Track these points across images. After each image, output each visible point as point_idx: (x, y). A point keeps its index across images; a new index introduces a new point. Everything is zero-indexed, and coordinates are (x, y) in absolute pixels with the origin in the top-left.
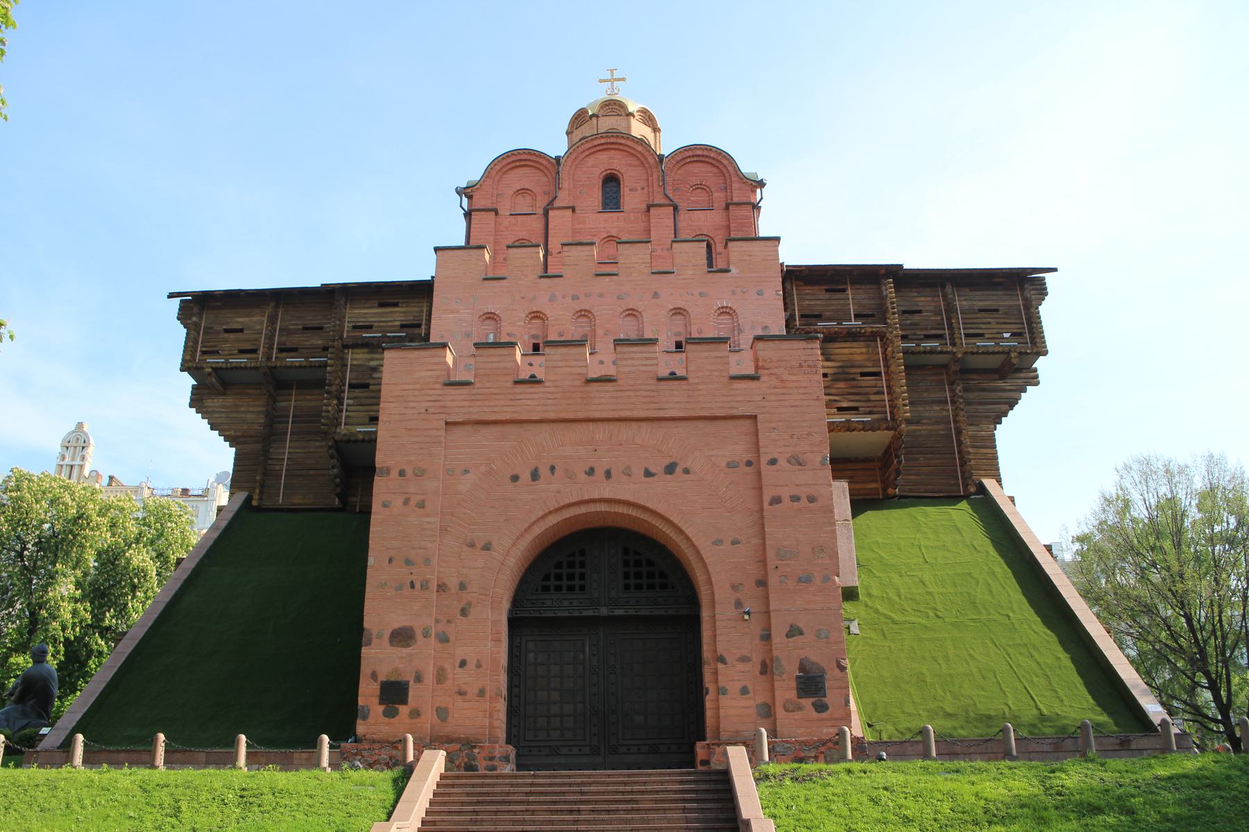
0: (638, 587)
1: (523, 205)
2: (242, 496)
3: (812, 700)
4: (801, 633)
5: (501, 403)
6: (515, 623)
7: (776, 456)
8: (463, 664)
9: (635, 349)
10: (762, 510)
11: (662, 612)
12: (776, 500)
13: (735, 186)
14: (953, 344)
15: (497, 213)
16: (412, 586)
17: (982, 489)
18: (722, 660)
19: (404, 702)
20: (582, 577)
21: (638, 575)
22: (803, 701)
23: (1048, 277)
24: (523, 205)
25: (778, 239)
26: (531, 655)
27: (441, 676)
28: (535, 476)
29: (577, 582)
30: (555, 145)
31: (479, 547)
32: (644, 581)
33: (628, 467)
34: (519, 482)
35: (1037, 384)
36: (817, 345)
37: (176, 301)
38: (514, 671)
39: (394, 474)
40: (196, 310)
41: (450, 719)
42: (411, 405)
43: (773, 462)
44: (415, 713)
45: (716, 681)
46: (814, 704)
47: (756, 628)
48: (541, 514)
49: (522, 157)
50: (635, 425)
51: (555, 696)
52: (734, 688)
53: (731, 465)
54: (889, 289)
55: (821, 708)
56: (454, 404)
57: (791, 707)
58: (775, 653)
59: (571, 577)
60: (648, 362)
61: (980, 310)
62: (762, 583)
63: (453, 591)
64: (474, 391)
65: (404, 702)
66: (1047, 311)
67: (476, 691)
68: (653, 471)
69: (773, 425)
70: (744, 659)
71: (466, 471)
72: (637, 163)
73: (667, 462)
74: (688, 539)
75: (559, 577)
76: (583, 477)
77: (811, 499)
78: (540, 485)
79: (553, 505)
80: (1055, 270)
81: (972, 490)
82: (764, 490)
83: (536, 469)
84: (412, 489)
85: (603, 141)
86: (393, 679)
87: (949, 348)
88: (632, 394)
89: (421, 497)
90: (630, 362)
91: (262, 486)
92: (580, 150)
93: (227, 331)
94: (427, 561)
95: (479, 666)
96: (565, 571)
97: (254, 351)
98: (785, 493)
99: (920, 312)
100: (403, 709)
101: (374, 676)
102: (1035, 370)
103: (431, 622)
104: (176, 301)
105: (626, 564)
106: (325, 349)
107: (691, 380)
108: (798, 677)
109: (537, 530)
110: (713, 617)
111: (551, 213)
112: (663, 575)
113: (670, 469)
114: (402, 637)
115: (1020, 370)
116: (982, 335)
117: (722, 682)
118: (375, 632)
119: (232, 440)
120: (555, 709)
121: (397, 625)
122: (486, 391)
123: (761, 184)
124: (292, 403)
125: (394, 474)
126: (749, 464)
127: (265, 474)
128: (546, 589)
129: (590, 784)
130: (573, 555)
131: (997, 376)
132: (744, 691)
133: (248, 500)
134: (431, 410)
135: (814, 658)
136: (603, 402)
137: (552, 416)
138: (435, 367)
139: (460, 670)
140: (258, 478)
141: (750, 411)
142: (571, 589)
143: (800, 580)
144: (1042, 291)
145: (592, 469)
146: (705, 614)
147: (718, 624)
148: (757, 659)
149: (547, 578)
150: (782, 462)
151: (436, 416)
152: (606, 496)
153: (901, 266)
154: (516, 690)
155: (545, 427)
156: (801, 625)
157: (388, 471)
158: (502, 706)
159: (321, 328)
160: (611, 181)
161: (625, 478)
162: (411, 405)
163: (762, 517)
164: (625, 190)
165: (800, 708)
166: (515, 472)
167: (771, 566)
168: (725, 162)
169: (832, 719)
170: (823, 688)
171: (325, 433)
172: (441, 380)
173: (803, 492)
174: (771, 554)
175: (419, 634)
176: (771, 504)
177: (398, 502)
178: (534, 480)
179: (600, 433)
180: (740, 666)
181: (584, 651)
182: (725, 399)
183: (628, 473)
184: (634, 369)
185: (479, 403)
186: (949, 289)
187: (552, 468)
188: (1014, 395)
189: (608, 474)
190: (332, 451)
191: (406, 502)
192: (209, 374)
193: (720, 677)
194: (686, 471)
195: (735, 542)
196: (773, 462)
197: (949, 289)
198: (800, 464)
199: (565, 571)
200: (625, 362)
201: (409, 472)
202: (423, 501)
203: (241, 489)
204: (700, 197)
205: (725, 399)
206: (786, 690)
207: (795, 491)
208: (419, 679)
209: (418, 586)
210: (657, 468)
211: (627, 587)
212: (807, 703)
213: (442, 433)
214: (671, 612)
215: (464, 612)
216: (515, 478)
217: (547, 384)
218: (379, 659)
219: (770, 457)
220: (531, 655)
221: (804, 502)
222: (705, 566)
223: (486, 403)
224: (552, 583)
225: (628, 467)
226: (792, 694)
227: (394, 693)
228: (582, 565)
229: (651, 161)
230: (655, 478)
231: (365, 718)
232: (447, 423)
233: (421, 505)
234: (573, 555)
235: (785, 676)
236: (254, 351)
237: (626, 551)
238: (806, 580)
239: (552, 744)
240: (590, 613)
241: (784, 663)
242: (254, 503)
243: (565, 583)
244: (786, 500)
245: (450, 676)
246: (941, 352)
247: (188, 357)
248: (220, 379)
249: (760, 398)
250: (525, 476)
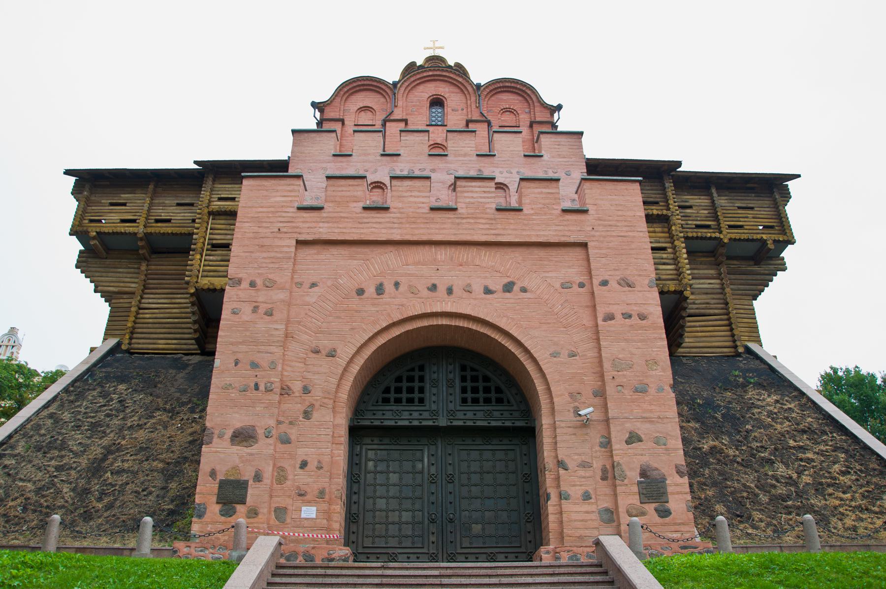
0: (475, 401)
1: (365, 118)
2: (112, 342)
3: (654, 505)
4: (640, 440)
5: (350, 225)
6: (356, 432)
7: (606, 278)
8: (304, 464)
9: (474, 184)
10: (597, 326)
11: (499, 424)
12: (610, 317)
13: (537, 109)
14: (721, 232)
15: (343, 124)
16: (257, 387)
17: (749, 351)
18: (561, 464)
19: (243, 502)
20: (422, 390)
21: (475, 390)
22: (646, 506)
23: (791, 184)
24: (365, 118)
25: (581, 133)
26: (371, 464)
27: (281, 476)
28: (380, 290)
29: (416, 395)
30: (392, 75)
31: (324, 352)
32: (481, 395)
33: (469, 285)
34: (366, 295)
35: (784, 269)
36: (637, 186)
37: (72, 180)
38: (354, 477)
39: (245, 285)
40: (87, 186)
41: (288, 520)
42: (264, 225)
43: (605, 283)
44: (253, 513)
45: (558, 486)
46: (656, 510)
47: (595, 435)
48: (384, 325)
49: (365, 83)
50: (474, 251)
51: (394, 504)
52: (576, 492)
53: (566, 286)
54: (669, 185)
55: (664, 513)
56: (308, 225)
57: (634, 512)
58: (616, 459)
59: (410, 390)
60: (486, 195)
61: (739, 208)
62: (601, 393)
63: (297, 394)
64: (324, 215)
65: (243, 502)
66: (792, 210)
67: (316, 492)
68: (492, 287)
69: (604, 251)
70: (584, 465)
71: (313, 285)
72: (457, 90)
73: (506, 280)
74: (526, 351)
75: (398, 390)
76: (425, 293)
77: (642, 317)
78: (385, 298)
79: (397, 317)
80: (799, 176)
81: (741, 350)
82: (598, 308)
83: (381, 285)
84: (260, 299)
85: (431, 73)
86: (232, 478)
87: (717, 235)
88: (472, 221)
89: (270, 306)
90: (470, 195)
91: (132, 333)
92: (412, 79)
93: (112, 204)
94: (273, 366)
95: (320, 468)
96: (405, 385)
97: (134, 221)
98: (617, 310)
99: (690, 207)
100: (240, 508)
101: (213, 474)
102: (783, 259)
103: (272, 422)
104: (72, 180)
105: (463, 379)
106: (194, 221)
107: (525, 211)
108: (639, 483)
109: (381, 340)
110: (554, 427)
111: (388, 124)
112: (498, 390)
113: (508, 288)
114: (243, 437)
115: (771, 258)
116: (741, 227)
117: (564, 487)
118: (216, 432)
119: (108, 297)
120: (394, 517)
121: (238, 425)
122: (335, 215)
123: (559, 107)
124: (165, 265)
125: (245, 285)
126: (582, 285)
127: (135, 322)
128: (386, 401)
129: (449, 576)
130: (413, 370)
131: (752, 263)
132: (587, 497)
133: (119, 344)
134: (285, 230)
135: (655, 465)
136: (444, 229)
137: (398, 238)
138: (289, 194)
139: (300, 471)
140: (129, 325)
141: (581, 238)
142: (410, 401)
143: (636, 391)
144: (786, 195)
146: (545, 421)
147: (558, 431)
148: (597, 465)
149: (387, 390)
150: (613, 284)
151: (288, 235)
152: (449, 308)
153: (679, 164)
154: (355, 498)
155: (390, 248)
156: (639, 433)
157: (239, 281)
158: (339, 510)
159: (192, 205)
160: (437, 102)
161: (466, 294)
162: (264, 225)
163: (597, 332)
164: (448, 110)
165: (643, 514)
166: (363, 286)
167: (608, 377)
168: (529, 92)
169: (675, 524)
170: (665, 493)
171: (188, 283)
172: (296, 205)
173: (634, 310)
174: (607, 365)
175: (260, 432)
176: (605, 320)
177: (247, 309)
178: (378, 294)
179: (442, 254)
180: (581, 473)
181: (422, 461)
182: (557, 228)
183: (468, 290)
184: (472, 200)
185: (326, 225)
186: (714, 191)
187: (397, 285)
188: (768, 277)
189: (450, 291)
190: (194, 299)
191: (255, 309)
192: (94, 238)
193: (561, 483)
194: (524, 290)
195: (572, 355)
196: (605, 283)
197: (714, 191)
198: (630, 286)
199: (405, 385)
200: (466, 195)
201: (259, 282)
202: (272, 309)
203: (114, 336)
204: (508, 119)
205: (557, 228)
206: (629, 497)
207: (626, 309)
208: (258, 478)
209: (262, 387)
210: (497, 284)
211: (464, 401)
212: (650, 508)
213: (293, 249)
214: (508, 424)
215: (307, 415)
216: (360, 292)
217: (391, 210)
218: (219, 457)
219: (601, 279)
220: (371, 464)
221: (635, 320)
222: (543, 375)
223: (335, 225)
224: (392, 396)
225: (469, 285)
226: (635, 500)
227: (232, 493)
228: (422, 379)
229: (469, 88)
230: (495, 296)
231: (200, 516)
232: (299, 243)
233: (269, 313)
234: (413, 370)
235: (626, 481)
236: (134, 221)
237: (463, 368)
238: (641, 390)
239: (390, 551)
240: (430, 423)
241: (624, 467)
242: (124, 347)
243: (404, 396)
244: (619, 316)
245: (290, 477)
246: (710, 238)
247: (77, 223)
248: (103, 243)
249: (590, 228)
250: (371, 291)
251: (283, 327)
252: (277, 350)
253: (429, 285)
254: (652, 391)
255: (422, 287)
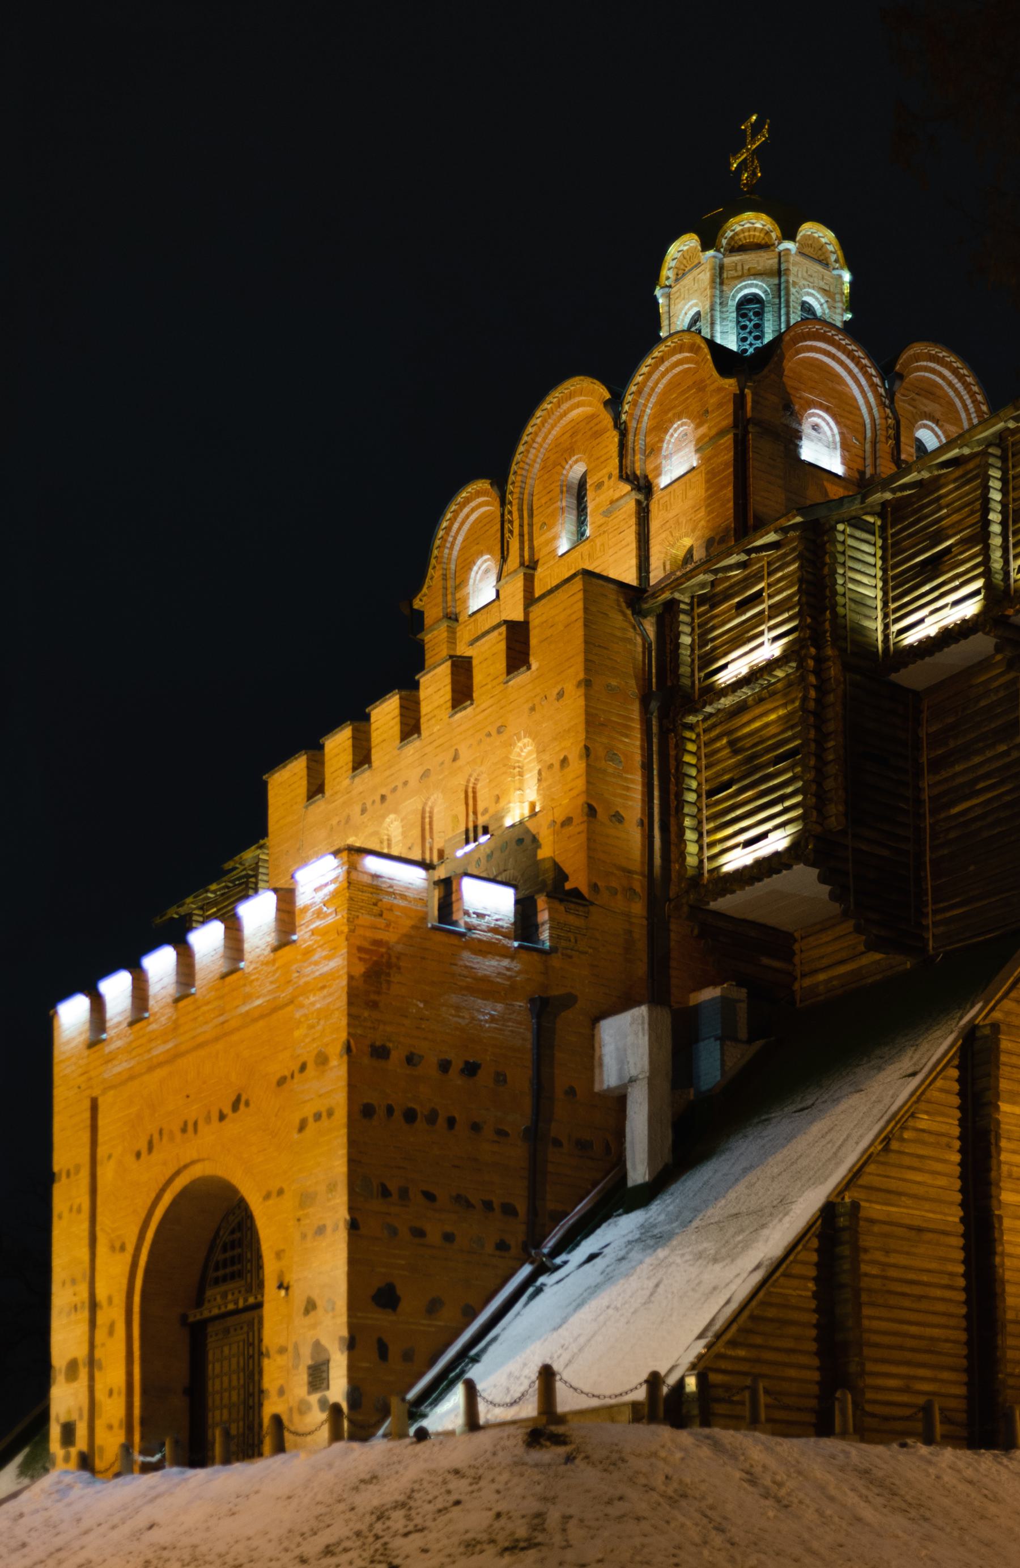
12: (302, 1127)
101: (57, 1420)
113: (235, 1106)
145: (186, 1123)
173: (321, 1106)
191: (71, 1210)
196: (303, 1068)
216: (138, 1155)
233: (79, 1211)
244: (311, 1120)
251: (85, 1225)
252: (86, 1258)
253: (181, 1125)
254: (329, 1230)
255: (176, 1128)
